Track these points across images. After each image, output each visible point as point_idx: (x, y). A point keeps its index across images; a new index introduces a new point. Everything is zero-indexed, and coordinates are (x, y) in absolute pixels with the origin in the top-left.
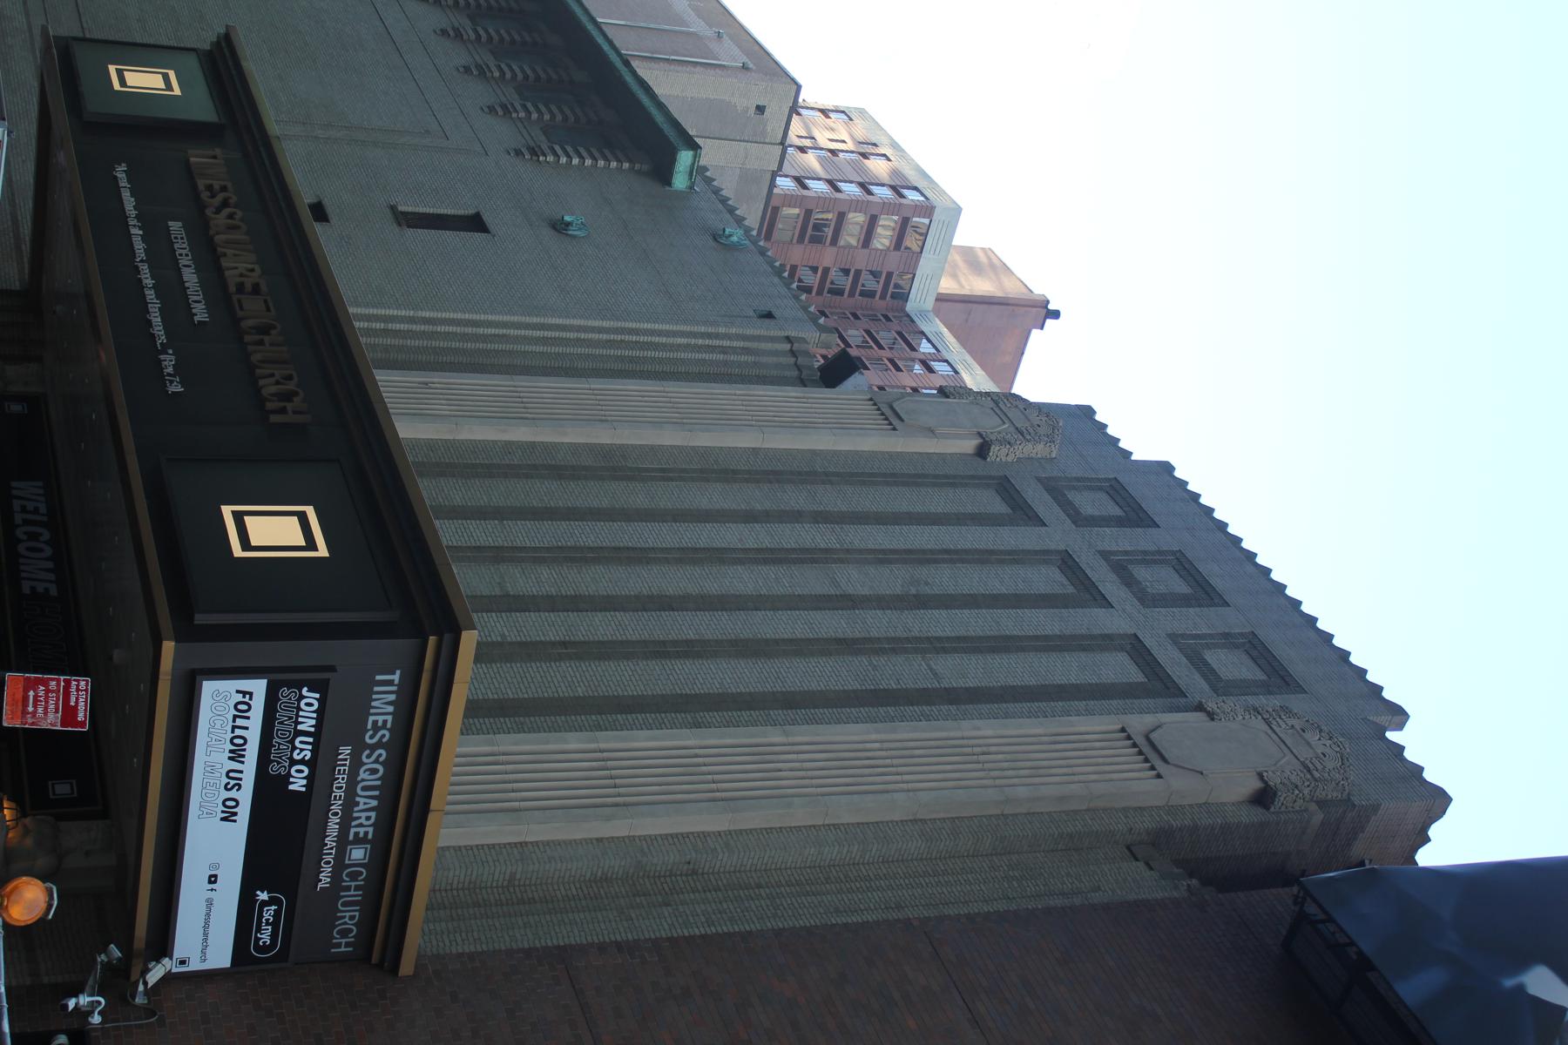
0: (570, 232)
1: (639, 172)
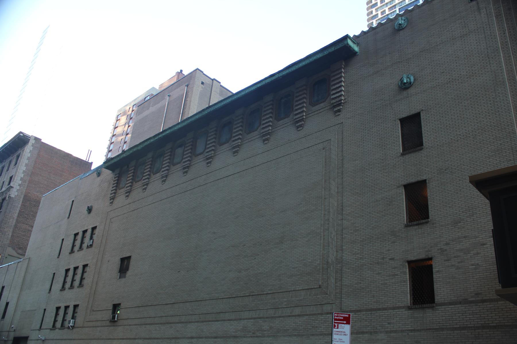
0: (412, 80)
1: (346, 65)
